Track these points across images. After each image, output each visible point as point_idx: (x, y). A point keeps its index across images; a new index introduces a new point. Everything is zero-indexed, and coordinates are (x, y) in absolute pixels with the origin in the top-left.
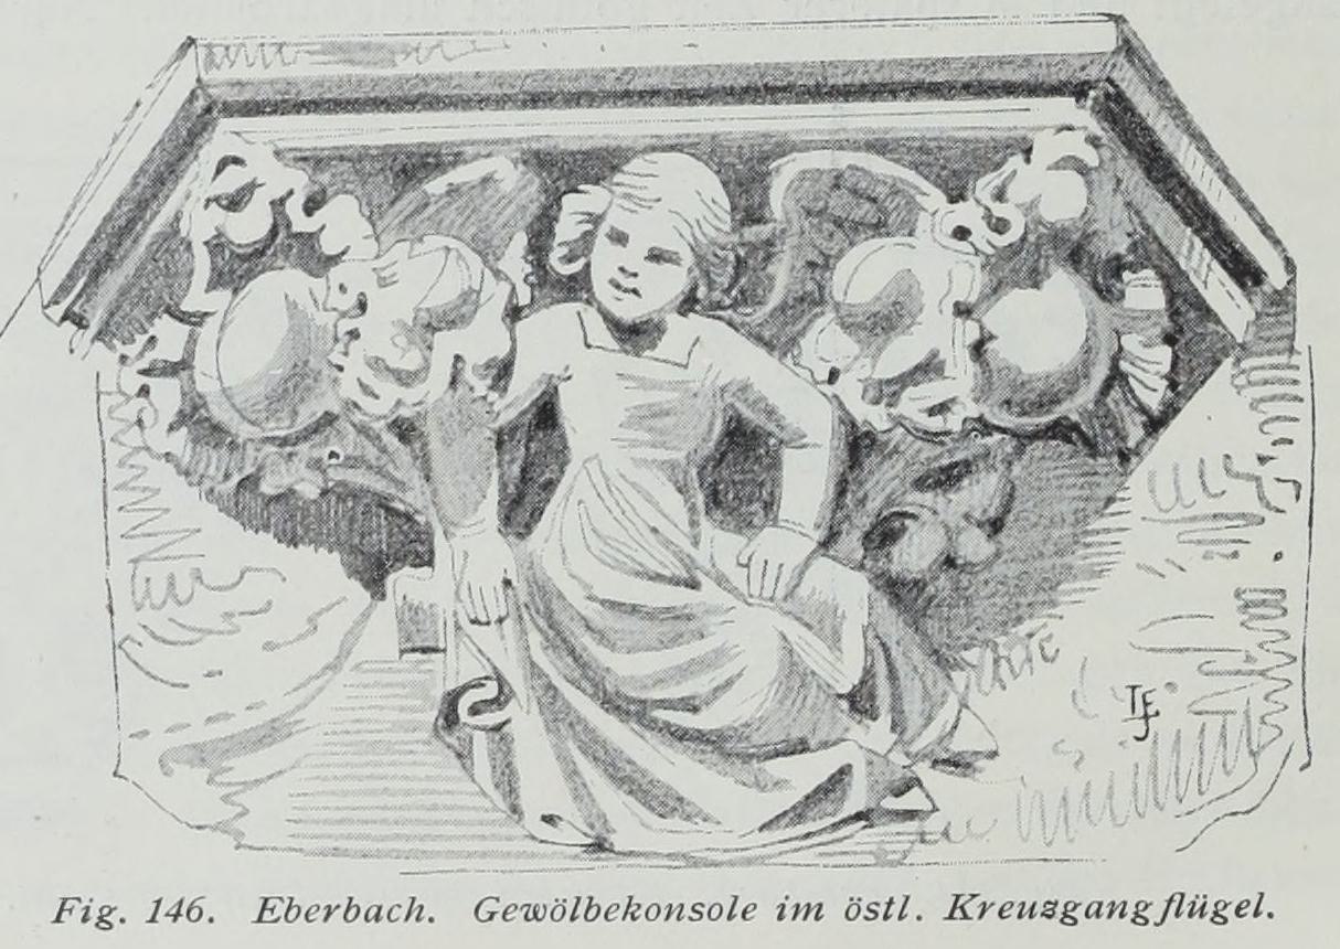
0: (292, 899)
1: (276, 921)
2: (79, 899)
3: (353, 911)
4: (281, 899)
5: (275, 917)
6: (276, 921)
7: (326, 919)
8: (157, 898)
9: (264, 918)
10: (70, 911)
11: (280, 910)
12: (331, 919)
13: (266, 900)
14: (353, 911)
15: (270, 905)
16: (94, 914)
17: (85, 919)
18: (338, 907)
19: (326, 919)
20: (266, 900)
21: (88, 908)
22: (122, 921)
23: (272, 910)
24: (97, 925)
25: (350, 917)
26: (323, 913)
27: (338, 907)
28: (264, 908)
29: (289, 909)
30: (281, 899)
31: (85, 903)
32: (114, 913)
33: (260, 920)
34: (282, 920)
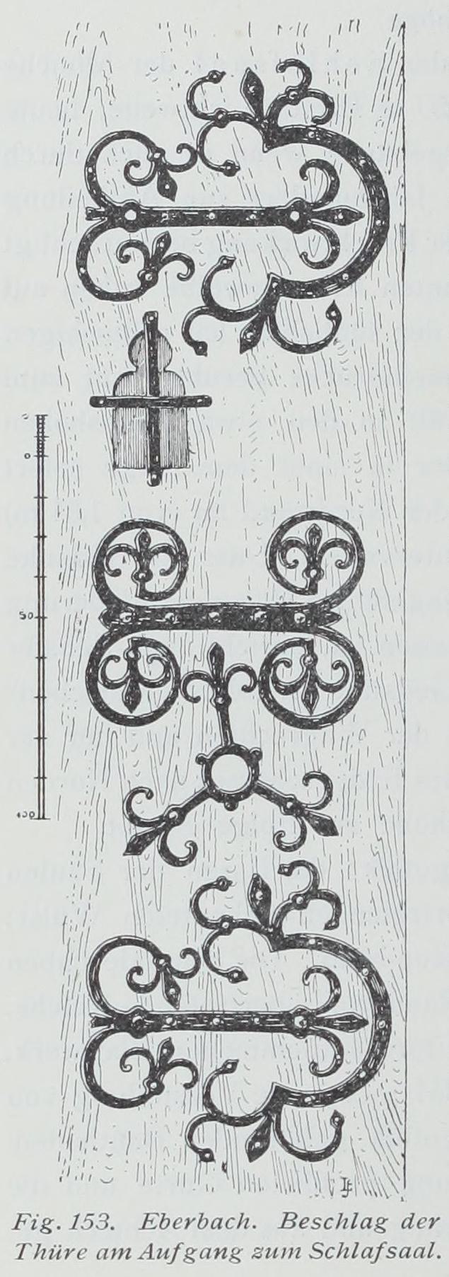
0: (164, 1214)
1: (154, 1228)
2: (30, 1215)
3: (204, 1222)
4: (157, 1214)
5: (152, 1226)
6: (154, 1228)
7: (186, 1227)
8: (76, 1214)
9: (146, 1227)
10: (24, 1222)
11: (157, 1220)
12: (190, 1227)
13: (148, 1215)
14: (204, 1222)
15: (149, 1218)
16: (39, 1225)
17: (33, 1228)
18: (194, 1219)
19: (186, 1227)
20: (148, 1215)
21: (35, 1221)
22: (59, 1228)
23: (152, 1221)
24: (41, 1231)
25: (201, 1226)
26: (185, 1223)
27: (194, 1219)
28: (146, 1220)
29: (163, 1220)
30: (157, 1214)
31: (34, 1217)
32: (52, 1223)
33: (144, 1228)
34: (158, 1226)
